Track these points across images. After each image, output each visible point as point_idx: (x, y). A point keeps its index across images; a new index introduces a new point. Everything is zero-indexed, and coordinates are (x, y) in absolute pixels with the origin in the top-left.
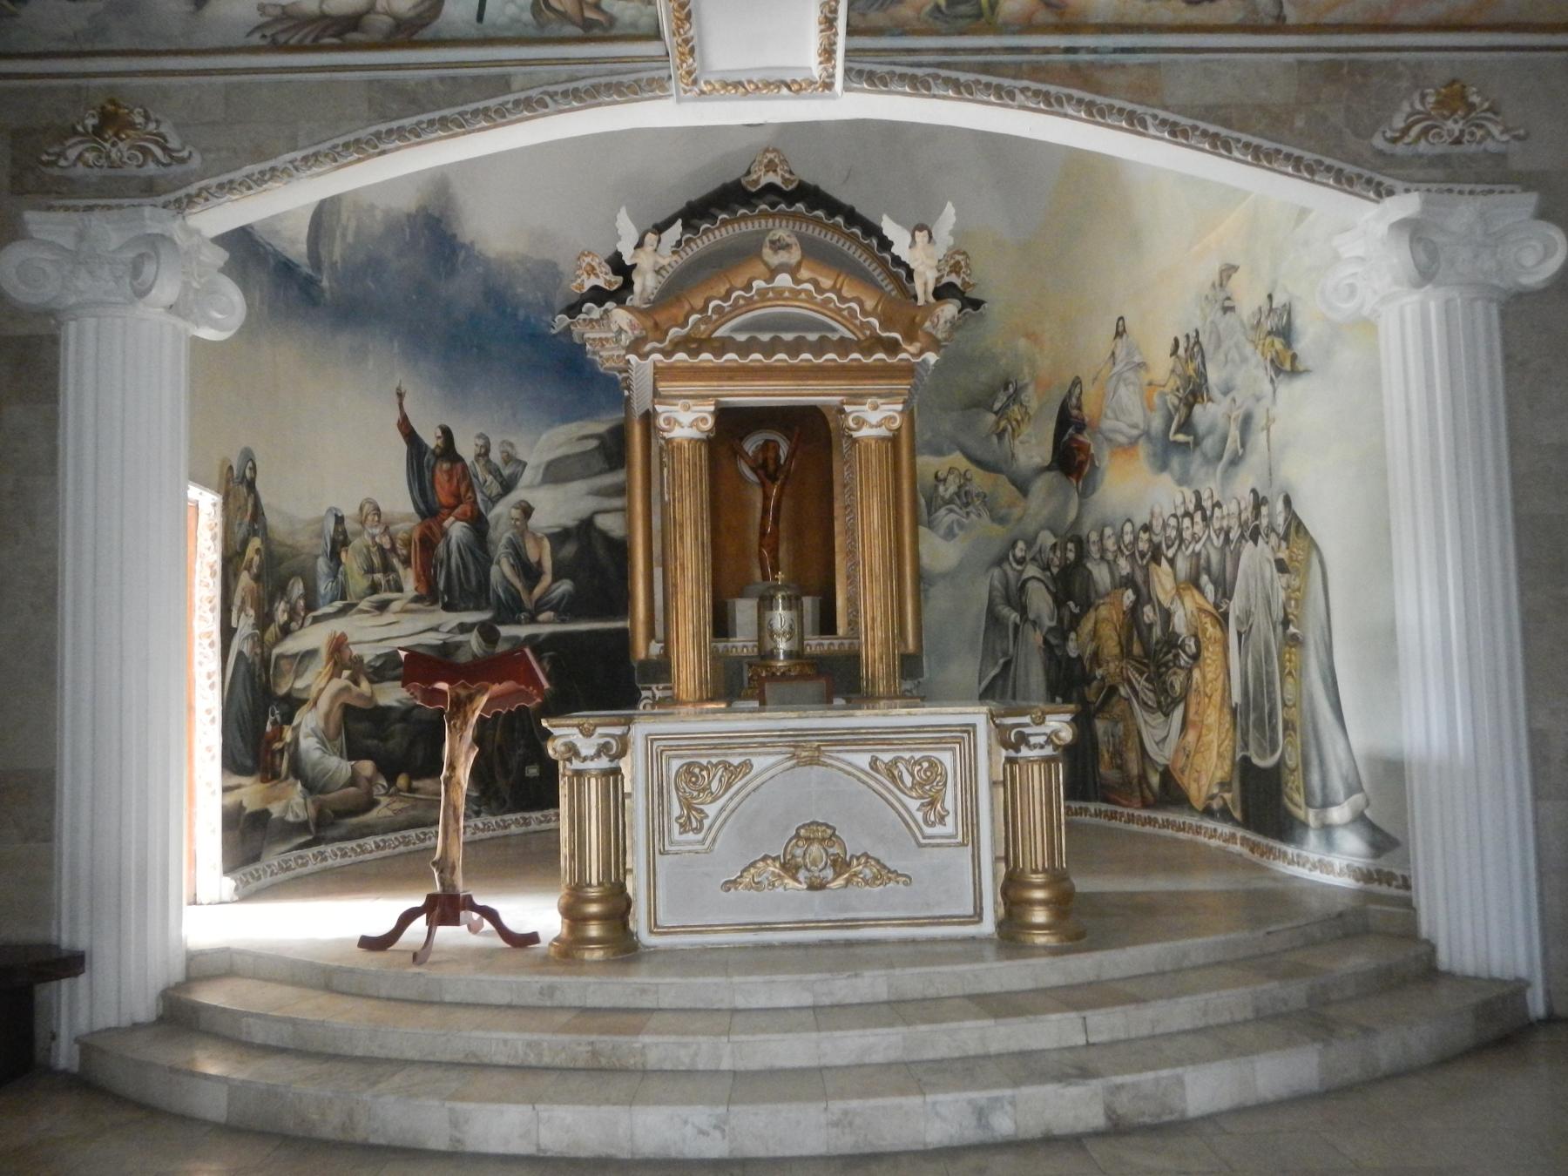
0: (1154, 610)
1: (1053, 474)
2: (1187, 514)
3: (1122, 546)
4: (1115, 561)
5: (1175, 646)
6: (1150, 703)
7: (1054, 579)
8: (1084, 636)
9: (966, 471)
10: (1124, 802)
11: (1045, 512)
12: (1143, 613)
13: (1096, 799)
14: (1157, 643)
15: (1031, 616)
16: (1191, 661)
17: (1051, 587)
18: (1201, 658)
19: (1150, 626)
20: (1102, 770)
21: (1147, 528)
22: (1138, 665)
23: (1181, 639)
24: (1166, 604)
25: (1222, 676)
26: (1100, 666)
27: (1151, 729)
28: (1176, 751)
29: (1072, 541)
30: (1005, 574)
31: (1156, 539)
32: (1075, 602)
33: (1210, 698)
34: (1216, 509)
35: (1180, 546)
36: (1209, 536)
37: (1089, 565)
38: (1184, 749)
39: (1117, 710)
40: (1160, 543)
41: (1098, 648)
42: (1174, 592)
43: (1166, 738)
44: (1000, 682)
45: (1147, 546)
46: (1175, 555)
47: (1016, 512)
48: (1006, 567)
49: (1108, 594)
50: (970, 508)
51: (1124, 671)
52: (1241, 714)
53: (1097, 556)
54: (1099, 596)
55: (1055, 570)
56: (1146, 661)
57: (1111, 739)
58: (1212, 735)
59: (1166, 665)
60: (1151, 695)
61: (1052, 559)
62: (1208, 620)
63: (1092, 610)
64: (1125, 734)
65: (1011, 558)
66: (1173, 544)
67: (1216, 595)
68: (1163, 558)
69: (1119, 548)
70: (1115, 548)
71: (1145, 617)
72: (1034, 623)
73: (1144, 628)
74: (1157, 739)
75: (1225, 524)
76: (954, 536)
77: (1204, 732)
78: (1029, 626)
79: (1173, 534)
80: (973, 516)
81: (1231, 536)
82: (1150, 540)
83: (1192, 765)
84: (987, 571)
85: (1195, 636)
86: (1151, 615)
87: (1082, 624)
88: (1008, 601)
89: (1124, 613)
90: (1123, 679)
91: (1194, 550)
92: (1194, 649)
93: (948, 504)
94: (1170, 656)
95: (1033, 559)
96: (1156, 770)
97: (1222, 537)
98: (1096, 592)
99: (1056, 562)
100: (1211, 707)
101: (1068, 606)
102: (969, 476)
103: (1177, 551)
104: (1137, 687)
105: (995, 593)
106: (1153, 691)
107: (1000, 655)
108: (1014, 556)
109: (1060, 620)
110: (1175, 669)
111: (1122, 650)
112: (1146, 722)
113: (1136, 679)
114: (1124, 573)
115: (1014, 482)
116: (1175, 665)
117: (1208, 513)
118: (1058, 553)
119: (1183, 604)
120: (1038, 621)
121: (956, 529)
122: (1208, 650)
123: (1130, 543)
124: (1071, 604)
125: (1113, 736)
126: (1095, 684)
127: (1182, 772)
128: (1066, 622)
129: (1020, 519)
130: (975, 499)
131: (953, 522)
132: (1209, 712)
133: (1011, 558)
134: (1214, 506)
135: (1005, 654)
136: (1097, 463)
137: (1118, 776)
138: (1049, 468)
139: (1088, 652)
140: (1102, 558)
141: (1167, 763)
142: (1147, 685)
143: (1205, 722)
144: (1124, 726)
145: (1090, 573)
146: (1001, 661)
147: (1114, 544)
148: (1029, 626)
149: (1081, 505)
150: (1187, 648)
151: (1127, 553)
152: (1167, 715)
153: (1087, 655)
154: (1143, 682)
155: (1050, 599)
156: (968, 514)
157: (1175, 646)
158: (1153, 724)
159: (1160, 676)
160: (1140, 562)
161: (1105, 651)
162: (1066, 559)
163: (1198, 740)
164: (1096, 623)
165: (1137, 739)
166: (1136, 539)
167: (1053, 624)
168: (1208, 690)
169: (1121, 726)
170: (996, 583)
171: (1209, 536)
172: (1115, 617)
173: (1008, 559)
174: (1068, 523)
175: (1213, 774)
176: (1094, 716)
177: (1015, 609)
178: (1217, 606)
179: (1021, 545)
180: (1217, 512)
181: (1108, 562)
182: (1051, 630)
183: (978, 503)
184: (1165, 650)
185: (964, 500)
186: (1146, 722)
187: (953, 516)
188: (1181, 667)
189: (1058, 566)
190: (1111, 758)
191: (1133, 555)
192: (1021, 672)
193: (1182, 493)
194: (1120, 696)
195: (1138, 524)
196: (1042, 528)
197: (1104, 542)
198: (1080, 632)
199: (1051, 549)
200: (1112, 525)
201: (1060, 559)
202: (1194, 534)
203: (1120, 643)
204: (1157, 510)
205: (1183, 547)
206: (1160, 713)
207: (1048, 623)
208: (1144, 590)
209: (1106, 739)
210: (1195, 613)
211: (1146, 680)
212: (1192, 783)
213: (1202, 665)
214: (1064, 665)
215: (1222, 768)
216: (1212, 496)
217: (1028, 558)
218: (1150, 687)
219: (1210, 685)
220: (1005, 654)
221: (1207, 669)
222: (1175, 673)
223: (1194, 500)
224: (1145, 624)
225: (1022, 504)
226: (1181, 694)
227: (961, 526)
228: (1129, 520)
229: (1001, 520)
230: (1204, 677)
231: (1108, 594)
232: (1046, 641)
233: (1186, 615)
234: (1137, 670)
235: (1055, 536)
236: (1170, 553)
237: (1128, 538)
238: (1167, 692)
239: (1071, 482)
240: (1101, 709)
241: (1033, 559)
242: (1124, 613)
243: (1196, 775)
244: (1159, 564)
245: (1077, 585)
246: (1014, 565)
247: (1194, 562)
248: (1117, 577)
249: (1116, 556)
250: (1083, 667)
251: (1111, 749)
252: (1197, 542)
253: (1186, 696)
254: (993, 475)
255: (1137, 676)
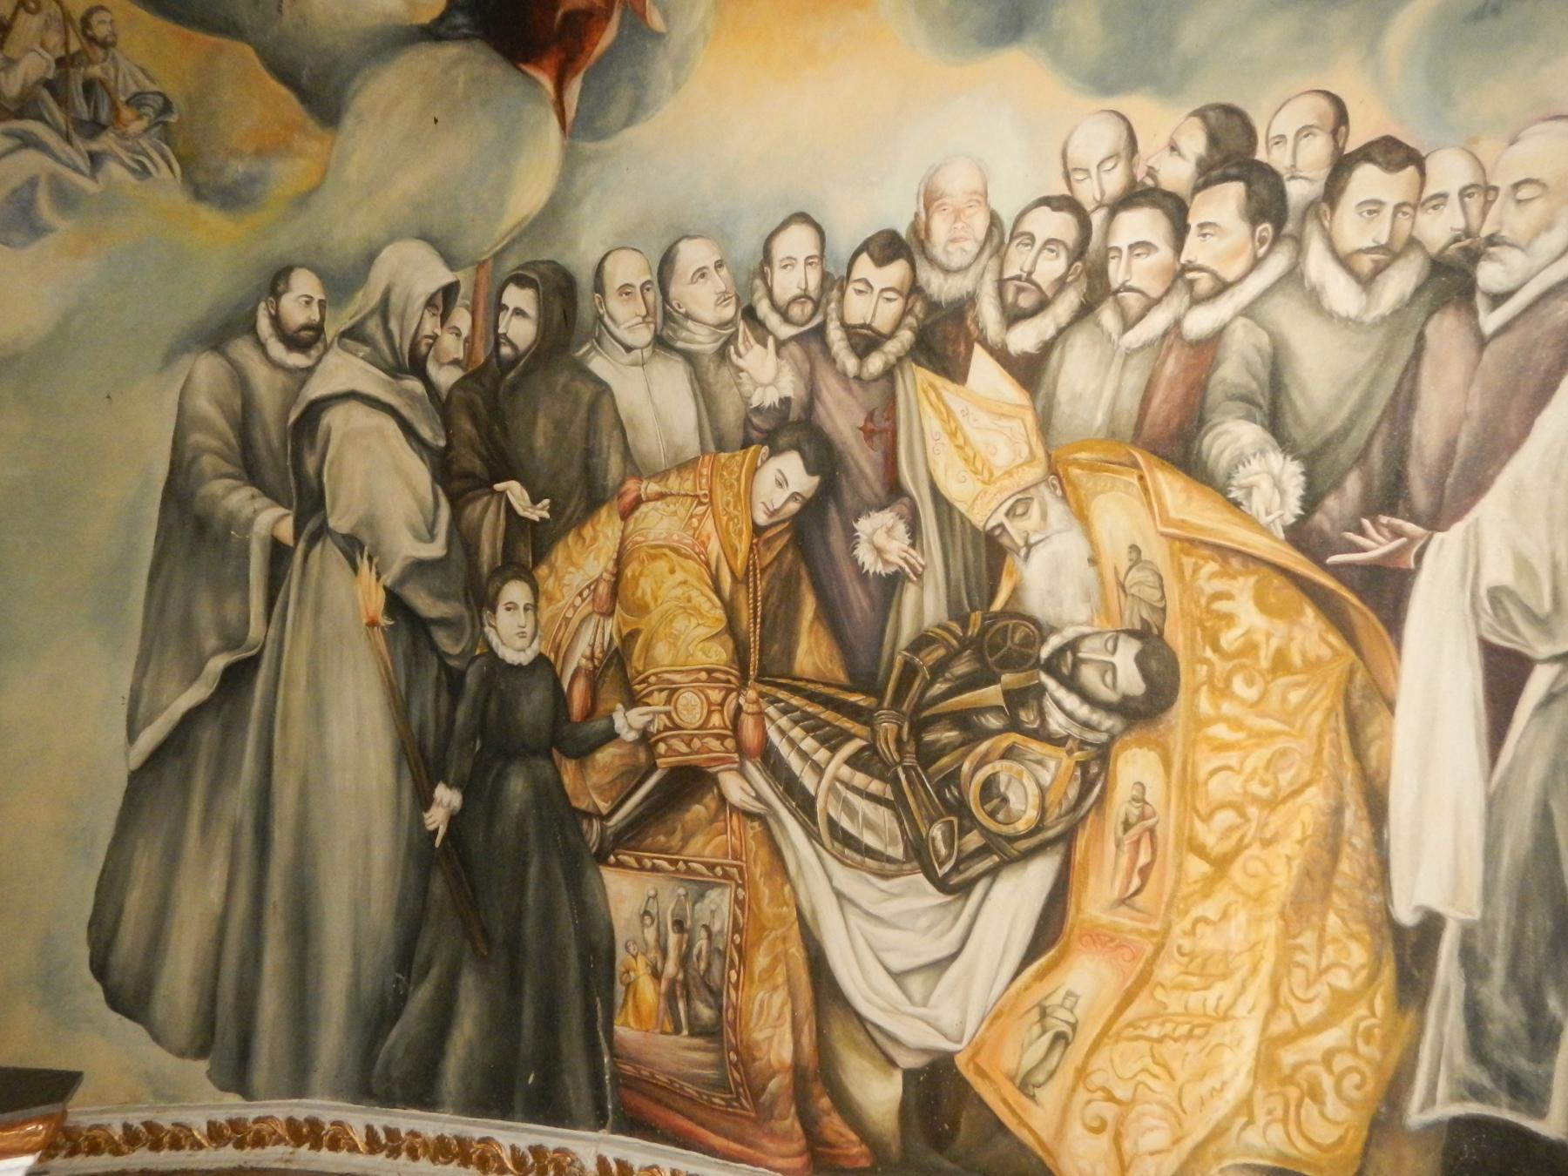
0: (914, 530)
1: (451, 51)
2: (1134, 196)
3: (763, 309)
4: (722, 354)
5: (1022, 659)
6: (869, 839)
7: (441, 405)
8: (566, 597)
9: (90, 12)
10: (719, 1142)
11: (410, 183)
12: (851, 537)
13: (600, 1121)
14: (922, 641)
15: (340, 522)
16: (1109, 723)
17: (426, 433)
18: (1178, 713)
19: (891, 584)
20: (626, 1031)
21: (888, 247)
22: (827, 715)
23: (1054, 642)
24: (982, 512)
25: (1315, 799)
26: (633, 701)
27: (855, 919)
28: (995, 1016)
29: (520, 281)
30: (241, 380)
31: (942, 287)
32: (526, 485)
33: (1221, 864)
34: (1367, 181)
35: (1086, 310)
36: (1294, 275)
37: (599, 365)
38: (1044, 1014)
39: (703, 848)
40: (971, 300)
41: (633, 635)
42: (1036, 472)
43: (953, 957)
44: (208, 736)
45: (896, 307)
46: (1047, 348)
47: (288, 175)
48: (242, 350)
49: (683, 466)
50: (106, 142)
51: (748, 724)
52: (1468, 955)
53: (643, 336)
54: (634, 466)
55: (445, 377)
56: (855, 698)
57: (673, 938)
58: (1222, 991)
59: (965, 721)
60: (883, 816)
61: (435, 337)
62: (1243, 587)
63: (604, 512)
64: (736, 928)
65: (264, 325)
66: (1043, 305)
67: (1312, 501)
68: (980, 358)
69: (750, 314)
70: (729, 311)
71: (865, 555)
72: (352, 547)
73: (859, 600)
74: (898, 963)
75: (1438, 229)
76: (36, 230)
77: (1167, 971)
78: (328, 556)
79: (1050, 268)
80: (114, 170)
81: (1489, 275)
82: (914, 289)
83: (1082, 1073)
84: (169, 358)
85: (1150, 638)
86: (897, 547)
87: (559, 555)
88: (249, 470)
89: (757, 530)
90: (740, 748)
91: (1178, 323)
92: (1130, 680)
93: (19, 115)
94: (992, 694)
95: (354, 334)
96: (892, 1063)
97: (1401, 281)
98: (627, 453)
99: (452, 346)
100: (1223, 895)
101: (502, 493)
102: (101, 31)
103: (1061, 332)
104: (808, 781)
105: (197, 438)
106: (898, 805)
107: (211, 642)
108: (276, 320)
109: (463, 539)
110: (1014, 738)
111: (740, 655)
112: (839, 895)
113: (804, 756)
114: (770, 397)
115: (286, 73)
116: (1014, 725)
117: (1298, 192)
118: (462, 319)
119: (1082, 517)
120: (365, 537)
121: (45, 208)
122: (1222, 690)
123: (804, 296)
124: (515, 491)
125: (679, 925)
126: (606, 756)
127: (1025, 1085)
128: (488, 549)
129: (303, 200)
130: (127, 113)
131: (33, 182)
132: (1210, 909)
133: (264, 325)
134: (1342, 166)
135: (232, 641)
136: (656, 20)
137: (709, 1057)
138: (433, 33)
139: (582, 647)
140: (661, 343)
141: (947, 1045)
142: (860, 779)
143: (1178, 937)
144: (739, 902)
145: (602, 388)
146: (217, 664)
147: (723, 299)
148: (328, 556)
149: (571, 162)
150: (1089, 676)
151: (786, 331)
152: (955, 888)
153: (579, 656)
154: (837, 766)
155: (421, 474)
156: (95, 159)
157: (1022, 659)
158: (888, 909)
159: (928, 756)
160: (850, 363)
161: (662, 651)
162: (498, 340)
163: (1128, 999)
164: (620, 561)
165: (797, 952)
166: (834, 283)
167: (435, 550)
168: (1209, 836)
169: (718, 906)
170: (204, 405)
171: (1294, 275)
172: (714, 547)
173: (252, 329)
174: (508, 223)
175: (1218, 1132)
176: (601, 858)
177: (277, 500)
178: (1300, 535)
179: (304, 284)
180: (1367, 181)
181: (690, 358)
182: (419, 568)
183: (136, 127)
184: (961, 668)
185: (84, 111)
186: (839, 895)
187: (31, 162)
188: (1058, 742)
189: (456, 362)
190: (671, 997)
191: (820, 331)
192: (295, 698)
193: (1123, 118)
194: (723, 800)
195: (848, 230)
196: (392, 239)
197: (675, 291)
198: (549, 585)
199: (430, 303)
200: (718, 234)
201: (469, 342)
202: (1180, 276)
203: (732, 627)
204: (957, 183)
205: (1108, 317)
206: (920, 877)
207: (406, 547)
208: (863, 459)
209: (650, 934)
210: (1156, 552)
211: (853, 762)
212: (1076, 1130)
213: (1177, 742)
214: (471, 680)
215: (1289, 1117)
216: (1342, 117)
217: (331, 332)
218: (876, 786)
219: (1225, 817)
220: (232, 641)
221: (1206, 763)
222: (1009, 753)
223: (1195, 143)
224: (862, 575)
225: (314, 147)
226: (1038, 828)
227: (65, 199)
228: (803, 218)
229: (231, 197)
230: (1188, 786)
231: (683, 466)
232: (395, 603)
233: (1093, 561)
234: (814, 727)
235: (450, 262)
236: (1024, 339)
237: (787, 283)
238: (960, 808)
239: (536, 84)
240: (633, 834)
241: (354, 334)
242: (757, 530)
243: (1109, 1111)
244: (954, 370)
245: (543, 425)
246: (277, 349)
247: (1170, 367)
248: (731, 414)
249: (732, 339)
250: (560, 700)
251: (671, 968)
252: (1196, 301)
253: (1067, 838)
254: (200, 37)
255: (808, 744)
